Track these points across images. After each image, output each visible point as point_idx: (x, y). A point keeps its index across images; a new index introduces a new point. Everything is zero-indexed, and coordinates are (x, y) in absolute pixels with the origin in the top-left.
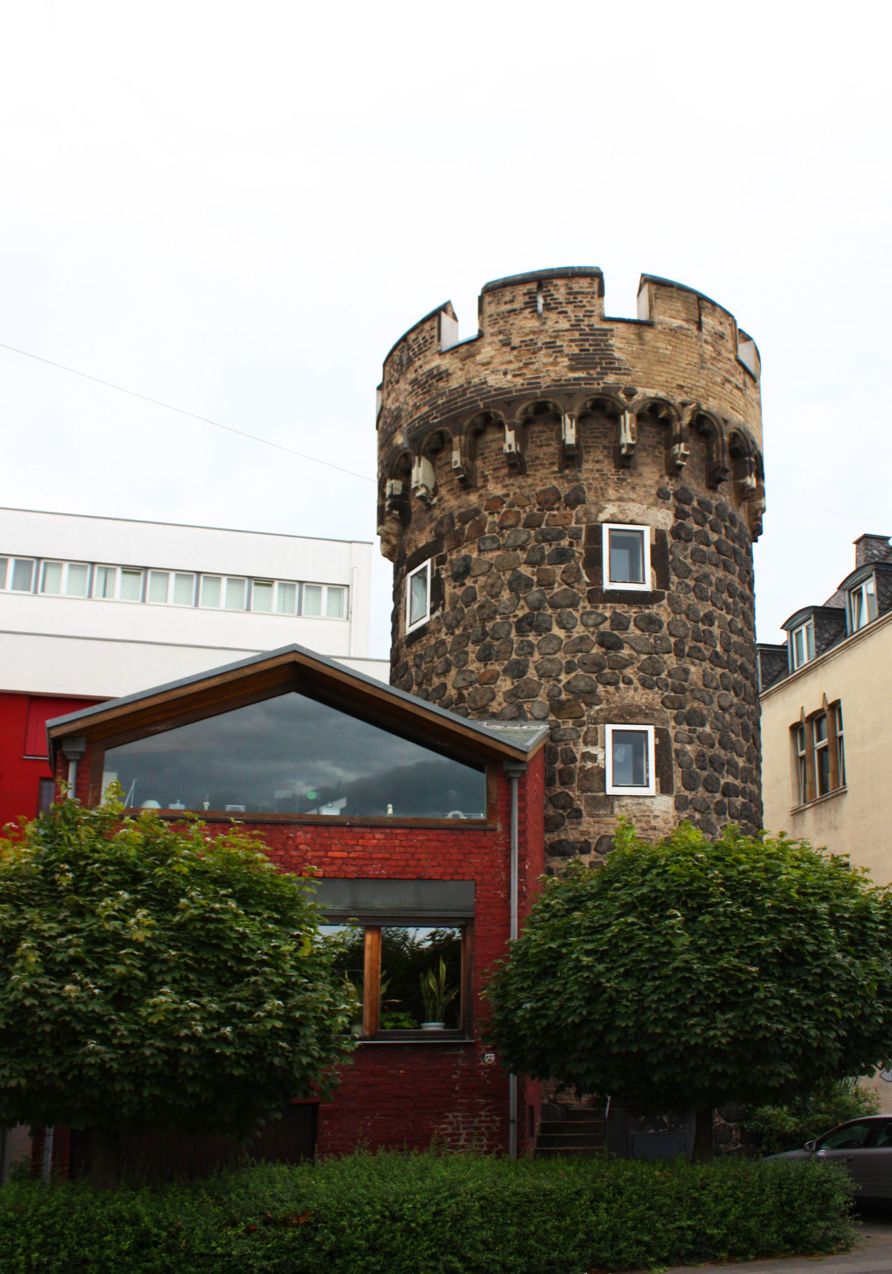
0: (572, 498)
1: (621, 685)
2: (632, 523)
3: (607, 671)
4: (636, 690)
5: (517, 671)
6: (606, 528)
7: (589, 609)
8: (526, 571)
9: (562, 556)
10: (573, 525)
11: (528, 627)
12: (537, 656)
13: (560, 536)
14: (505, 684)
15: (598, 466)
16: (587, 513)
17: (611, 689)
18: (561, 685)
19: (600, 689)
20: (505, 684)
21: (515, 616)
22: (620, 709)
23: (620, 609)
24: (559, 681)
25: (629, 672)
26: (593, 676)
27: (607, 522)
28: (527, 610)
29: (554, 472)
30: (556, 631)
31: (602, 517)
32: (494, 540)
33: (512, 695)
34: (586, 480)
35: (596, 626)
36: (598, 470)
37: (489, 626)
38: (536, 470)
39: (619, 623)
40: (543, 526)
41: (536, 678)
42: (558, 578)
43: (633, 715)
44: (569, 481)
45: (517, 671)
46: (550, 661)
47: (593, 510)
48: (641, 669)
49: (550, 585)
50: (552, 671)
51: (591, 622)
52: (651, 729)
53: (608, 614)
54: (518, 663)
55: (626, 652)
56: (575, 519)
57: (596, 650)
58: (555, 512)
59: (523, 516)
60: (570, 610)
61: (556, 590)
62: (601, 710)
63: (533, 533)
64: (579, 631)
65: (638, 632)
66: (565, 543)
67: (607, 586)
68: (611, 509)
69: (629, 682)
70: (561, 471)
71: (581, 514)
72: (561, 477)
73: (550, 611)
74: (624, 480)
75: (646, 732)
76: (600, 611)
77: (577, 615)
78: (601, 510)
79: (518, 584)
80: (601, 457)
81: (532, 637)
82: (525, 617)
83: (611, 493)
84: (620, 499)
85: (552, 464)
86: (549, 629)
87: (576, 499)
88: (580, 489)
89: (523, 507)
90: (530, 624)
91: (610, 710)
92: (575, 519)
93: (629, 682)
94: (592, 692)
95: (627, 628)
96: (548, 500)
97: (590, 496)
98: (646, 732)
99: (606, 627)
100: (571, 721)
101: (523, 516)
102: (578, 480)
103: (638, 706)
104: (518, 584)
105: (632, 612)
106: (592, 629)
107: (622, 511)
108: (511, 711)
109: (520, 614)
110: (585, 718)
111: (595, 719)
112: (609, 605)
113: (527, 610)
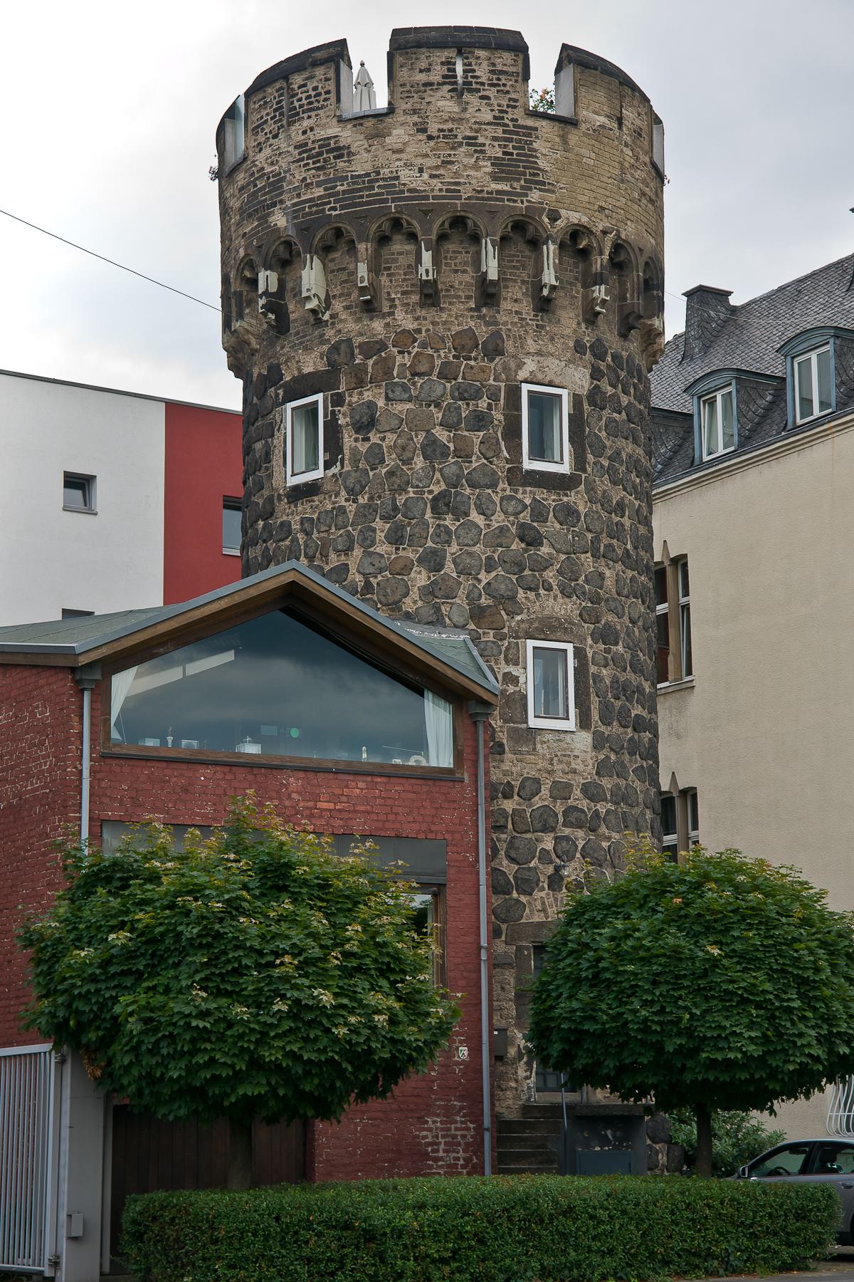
0: (490, 347)
1: (542, 591)
2: (550, 384)
3: (527, 572)
4: (555, 598)
5: (433, 561)
6: (525, 388)
7: (508, 493)
8: (442, 435)
9: (480, 420)
10: (491, 382)
11: (445, 509)
12: (454, 548)
13: (477, 395)
14: (420, 578)
15: (516, 307)
16: (506, 368)
17: (532, 595)
18: (481, 587)
19: (521, 594)
20: (420, 578)
21: (430, 492)
22: (541, 620)
23: (541, 494)
24: (479, 581)
25: (550, 575)
26: (514, 578)
27: (526, 381)
28: (444, 487)
29: (471, 310)
30: (475, 516)
31: (522, 375)
32: (405, 388)
33: (428, 591)
34: (505, 324)
35: (516, 514)
36: (517, 312)
37: (401, 499)
38: (450, 303)
39: (539, 512)
40: (460, 380)
41: (454, 575)
42: (476, 450)
43: (553, 629)
44: (487, 324)
45: (433, 561)
46: (470, 554)
47: (513, 365)
48: (560, 572)
49: (468, 457)
50: (471, 567)
51: (511, 509)
52: (569, 647)
53: (528, 501)
54: (434, 552)
55: (545, 550)
56: (492, 374)
57: (517, 546)
58: (472, 363)
59: (438, 362)
60: (489, 491)
61: (474, 465)
62: (522, 621)
63: (448, 385)
64: (498, 519)
65: (558, 526)
66: (483, 404)
67: (528, 464)
68: (530, 365)
69: (549, 589)
70: (478, 309)
71: (499, 368)
72: (479, 317)
73: (468, 491)
74: (543, 327)
75: (565, 651)
76: (520, 496)
77: (497, 499)
78: (520, 365)
79: (433, 450)
80: (519, 296)
81: (448, 521)
82: (442, 495)
83: (531, 345)
84: (539, 353)
85: (469, 297)
86: (467, 514)
87: (494, 350)
88: (497, 335)
89: (437, 350)
90: (447, 505)
91: (531, 622)
92: (492, 374)
93: (549, 589)
94: (513, 598)
95: (546, 520)
96: (464, 344)
97: (509, 346)
98: (565, 651)
99: (525, 517)
100: (491, 632)
101: (438, 362)
102: (496, 323)
103: (558, 619)
104: (433, 450)
105: (550, 499)
106: (512, 518)
107: (541, 369)
108: (427, 613)
109: (437, 490)
110: (505, 630)
111: (516, 632)
112: (528, 489)
113: (444, 487)
